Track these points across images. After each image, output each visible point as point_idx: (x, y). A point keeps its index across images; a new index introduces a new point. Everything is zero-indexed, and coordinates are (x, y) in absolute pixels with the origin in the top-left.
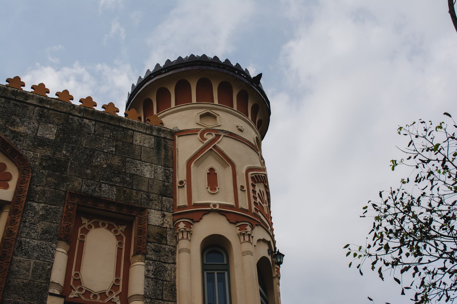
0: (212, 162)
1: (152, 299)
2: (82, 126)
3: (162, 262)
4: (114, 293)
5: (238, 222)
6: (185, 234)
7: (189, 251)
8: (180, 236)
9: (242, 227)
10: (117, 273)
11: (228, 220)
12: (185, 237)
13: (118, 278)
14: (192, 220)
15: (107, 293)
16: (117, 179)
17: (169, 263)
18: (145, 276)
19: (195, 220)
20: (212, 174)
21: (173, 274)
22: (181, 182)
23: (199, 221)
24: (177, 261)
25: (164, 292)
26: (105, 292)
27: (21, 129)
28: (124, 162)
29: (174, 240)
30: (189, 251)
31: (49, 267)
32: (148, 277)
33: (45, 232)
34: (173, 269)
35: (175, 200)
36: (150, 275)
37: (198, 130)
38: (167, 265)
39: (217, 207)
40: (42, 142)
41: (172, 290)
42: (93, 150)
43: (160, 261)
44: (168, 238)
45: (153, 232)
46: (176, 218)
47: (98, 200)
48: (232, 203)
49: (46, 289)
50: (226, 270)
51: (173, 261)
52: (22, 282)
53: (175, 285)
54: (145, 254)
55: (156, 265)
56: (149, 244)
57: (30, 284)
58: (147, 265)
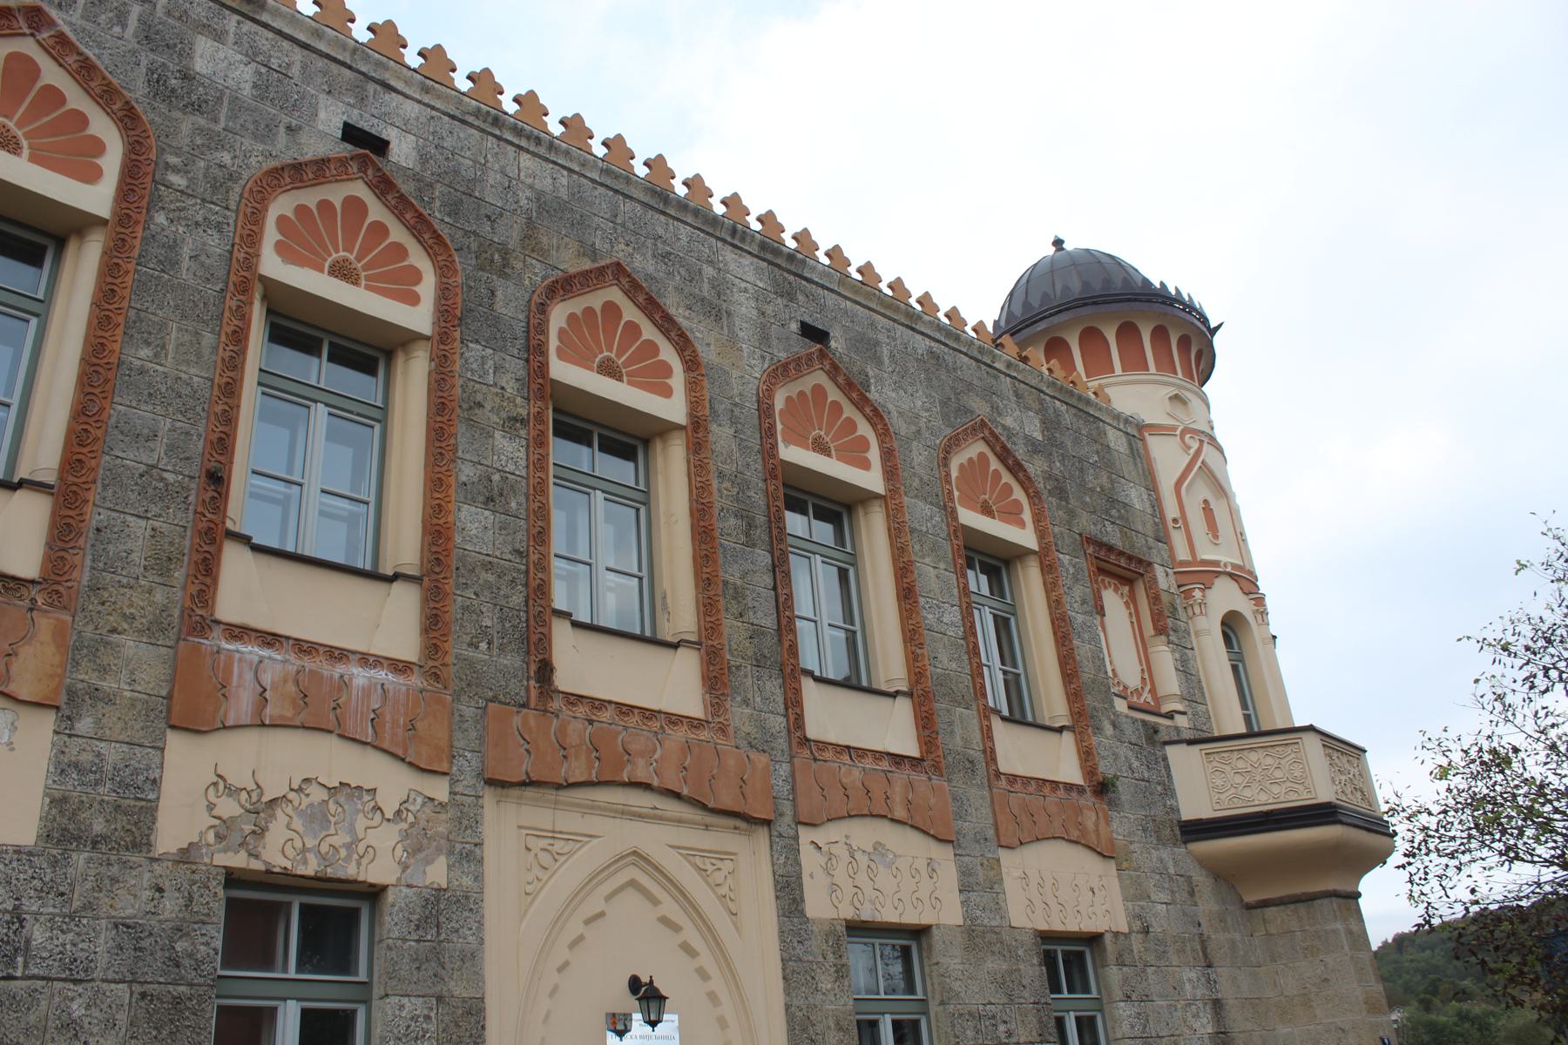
0: (1203, 492)
2: (1057, 413)
8: (1197, 610)
16: (1114, 512)
20: (1207, 510)
22: (1175, 521)
27: (1008, 421)
28: (1112, 482)
33: (1084, 602)
35: (1171, 549)
37: (1174, 428)
39: (1229, 569)
40: (1035, 448)
42: (1081, 460)
47: (1110, 548)
48: (1239, 562)
58: (1173, 651)
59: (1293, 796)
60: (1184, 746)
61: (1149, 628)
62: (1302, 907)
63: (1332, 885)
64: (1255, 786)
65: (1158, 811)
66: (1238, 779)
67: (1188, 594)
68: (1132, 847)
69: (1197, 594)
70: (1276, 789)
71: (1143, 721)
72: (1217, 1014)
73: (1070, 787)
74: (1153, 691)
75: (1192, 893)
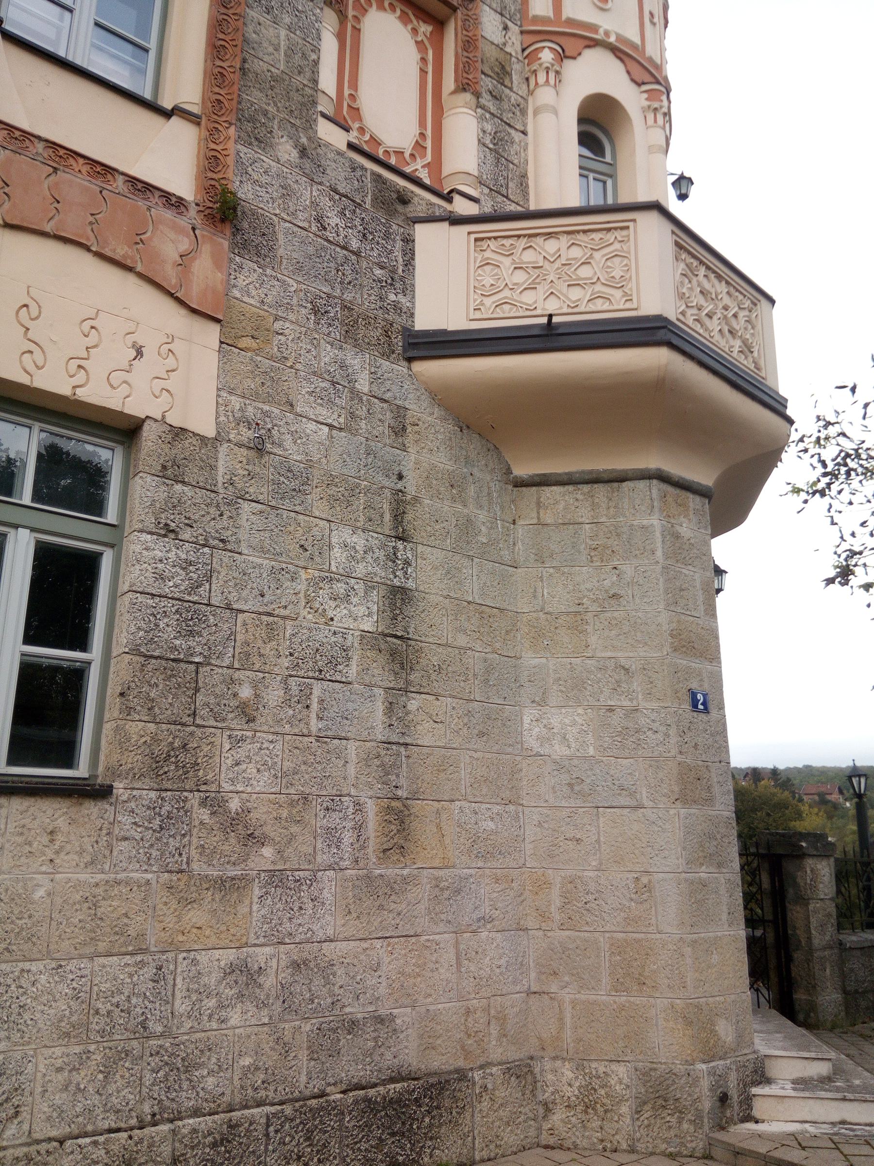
1: (491, 190)
3: (506, 123)
4: (418, 159)
5: (644, 83)
6: (552, 75)
7: (556, 113)
8: (542, 77)
9: (652, 95)
10: (422, 123)
11: (628, 72)
12: (552, 81)
13: (424, 132)
14: (563, 51)
15: (407, 155)
17: (516, 129)
18: (479, 140)
19: (567, 54)
21: (523, 154)
23: (574, 58)
24: (530, 129)
25: (511, 184)
26: (403, 153)
29: (525, 87)
30: (556, 113)
31: (314, 56)
32: (484, 145)
34: (523, 144)
36: (488, 142)
38: (512, 132)
41: (522, 185)
43: (502, 120)
44: (514, 77)
45: (488, 55)
46: (530, 39)
49: (314, 103)
50: (610, 176)
51: (522, 129)
52: (268, 71)
53: (524, 176)
54: (477, 95)
55: (495, 124)
56: (483, 76)
57: (284, 80)
58: (482, 118)
59: (599, 305)
60: (446, 224)
61: (449, 82)
62: (601, 490)
63: (652, 462)
64: (542, 290)
65: (365, 300)
66: (520, 277)
67: (532, 57)
68: (278, 325)
69: (547, 56)
70: (575, 294)
71: (378, 178)
72: (393, 605)
73: (141, 187)
74: (436, 166)
75: (399, 431)
